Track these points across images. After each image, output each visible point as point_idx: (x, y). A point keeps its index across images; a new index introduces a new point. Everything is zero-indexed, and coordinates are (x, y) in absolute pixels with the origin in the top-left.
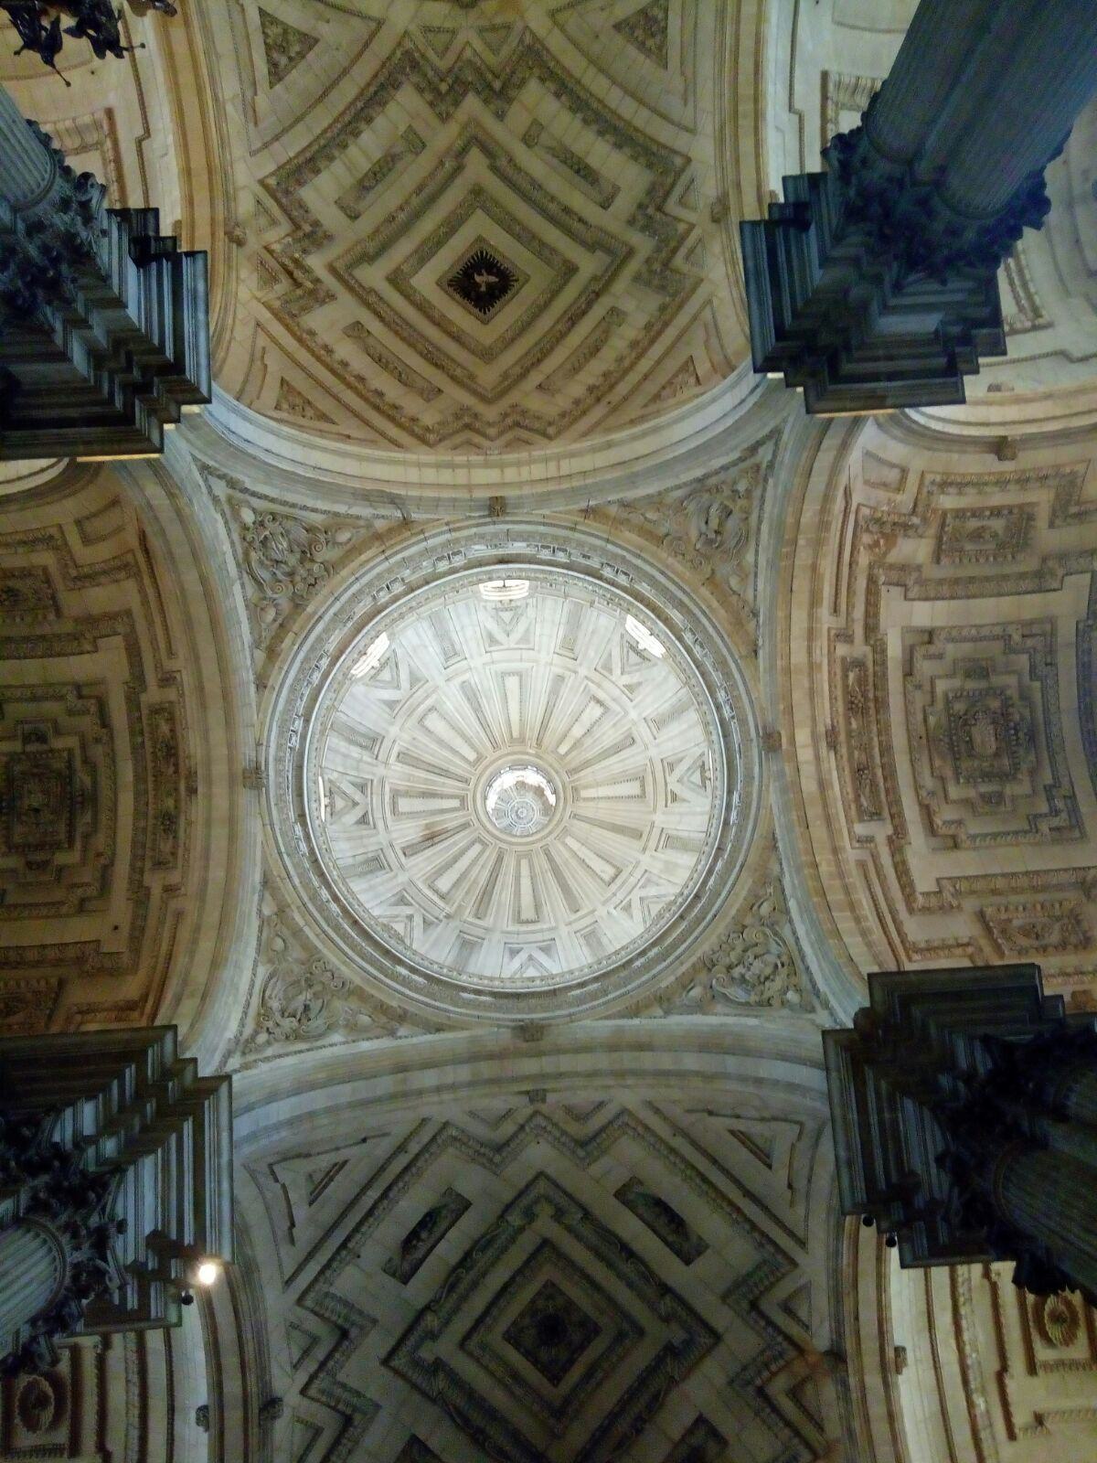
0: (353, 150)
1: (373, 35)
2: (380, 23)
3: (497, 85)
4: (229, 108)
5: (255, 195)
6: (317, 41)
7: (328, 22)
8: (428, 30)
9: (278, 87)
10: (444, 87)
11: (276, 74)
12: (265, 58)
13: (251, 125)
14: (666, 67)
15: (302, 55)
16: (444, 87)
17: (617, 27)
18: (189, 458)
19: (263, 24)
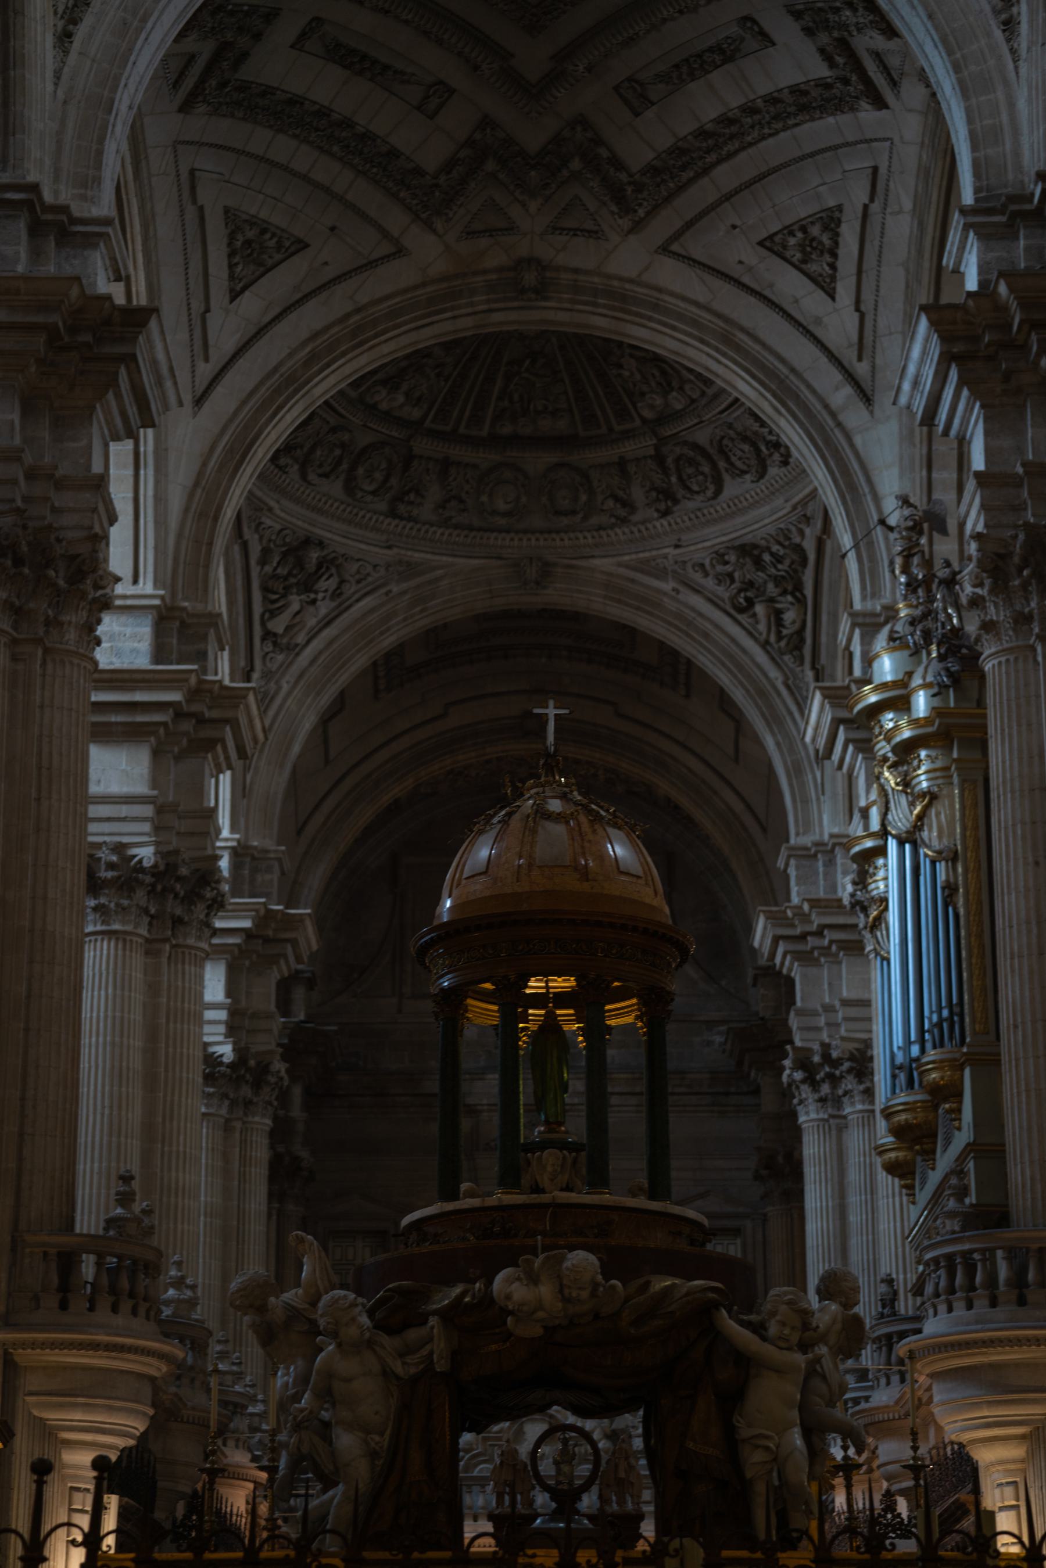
0: (735, 101)
1: (677, 236)
2: (665, 249)
3: (490, 166)
4: (908, 205)
5: (898, 96)
6: (761, 243)
7: (740, 262)
8: (594, 234)
9: (832, 203)
10: (576, 164)
11: (831, 220)
12: (840, 240)
13: (883, 171)
14: (227, 210)
15: (789, 230)
16: (576, 164)
17: (302, 245)
18: (1023, 70)
19: (833, 278)
